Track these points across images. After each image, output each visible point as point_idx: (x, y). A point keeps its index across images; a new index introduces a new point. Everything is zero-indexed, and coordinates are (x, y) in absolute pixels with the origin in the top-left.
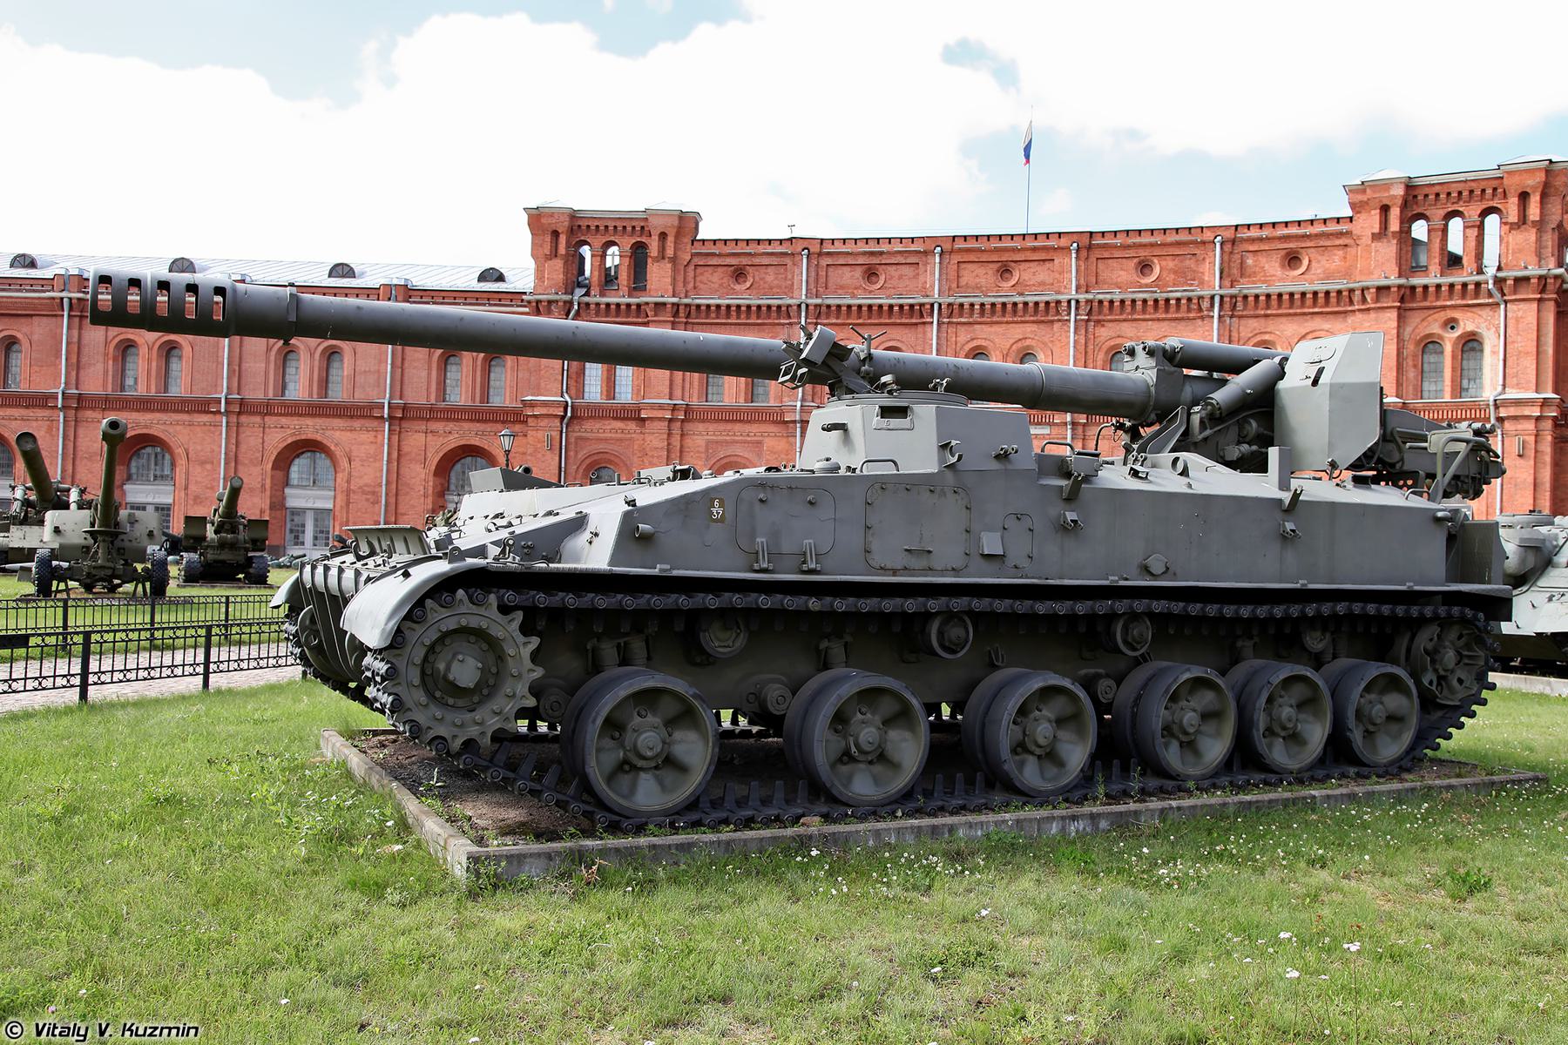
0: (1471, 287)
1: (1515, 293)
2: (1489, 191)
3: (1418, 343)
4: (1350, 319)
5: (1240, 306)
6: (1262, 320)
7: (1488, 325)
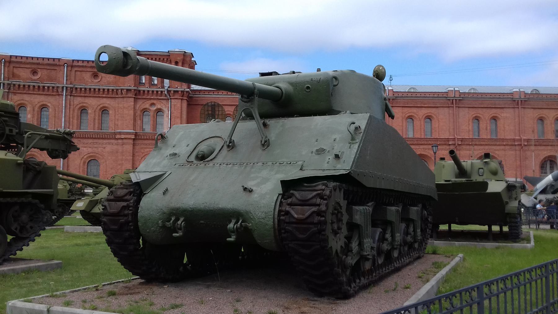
0: (159, 92)
1: (174, 96)
2: (165, 59)
3: (141, 111)
4: (117, 100)
5: (74, 91)
6: (83, 98)
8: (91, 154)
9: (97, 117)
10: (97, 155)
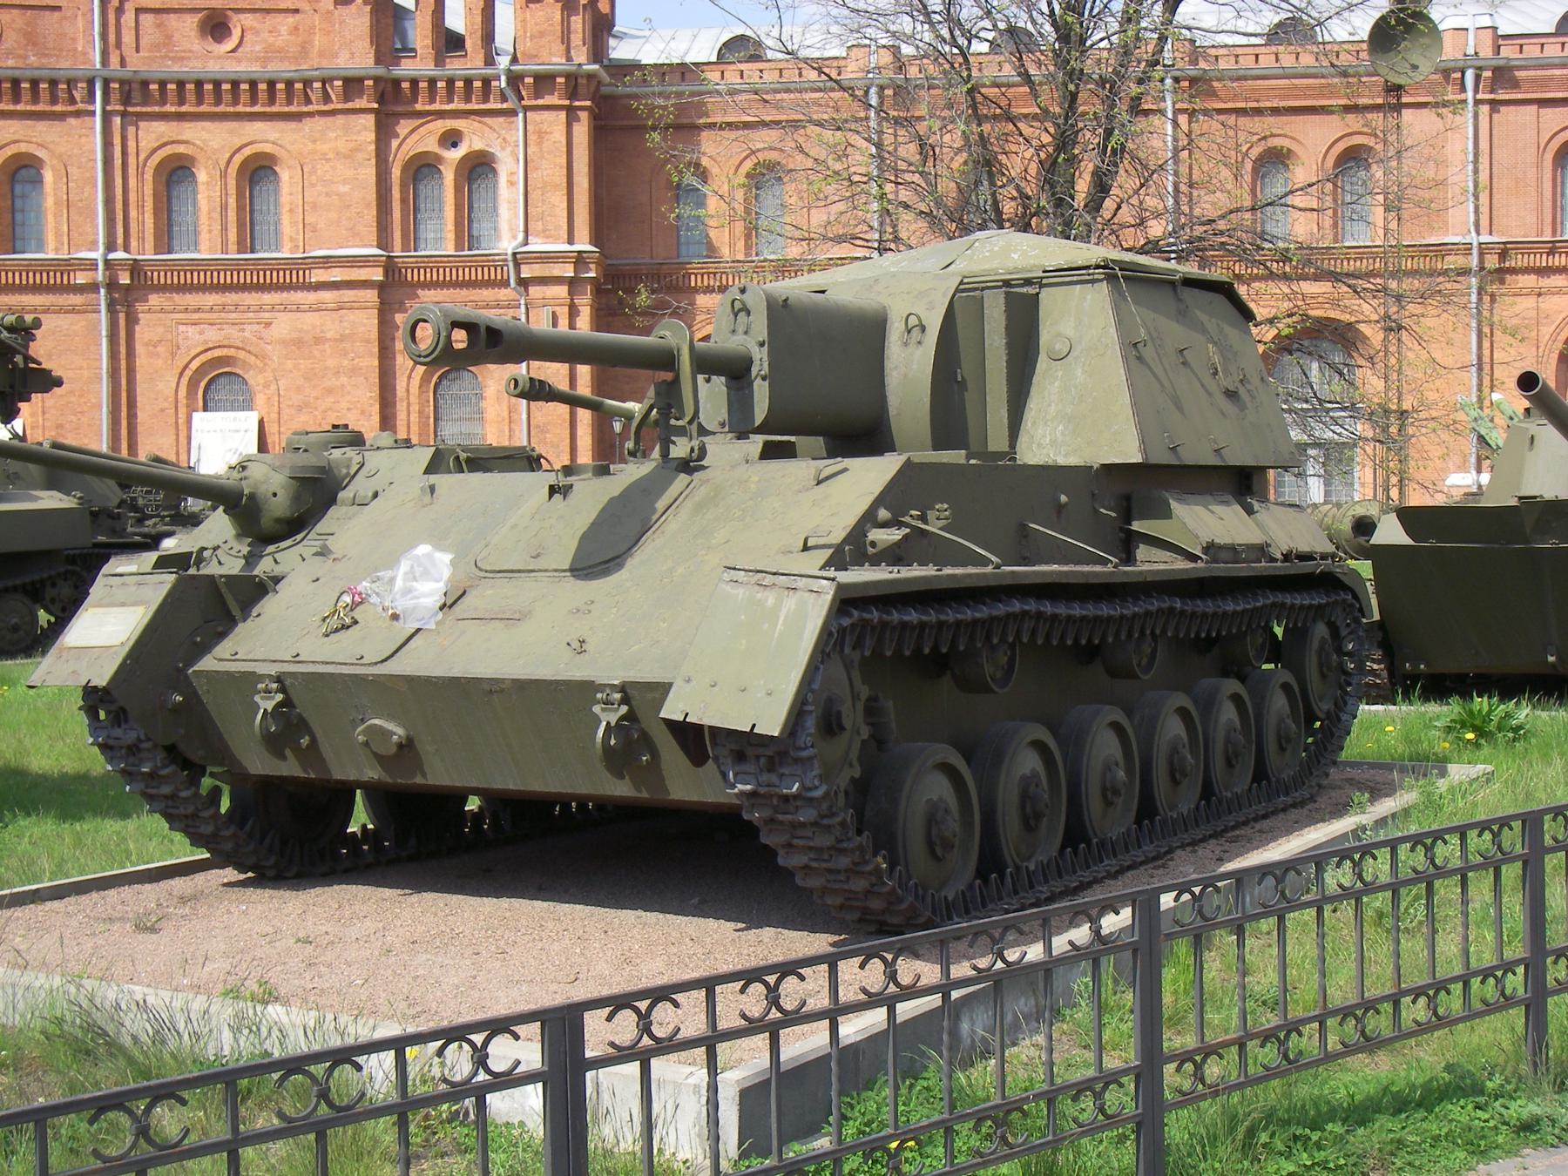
4: (308, 124)
5: (136, 96)
7: (501, 140)
8: (217, 353)
9: (232, 201)
10: (241, 355)
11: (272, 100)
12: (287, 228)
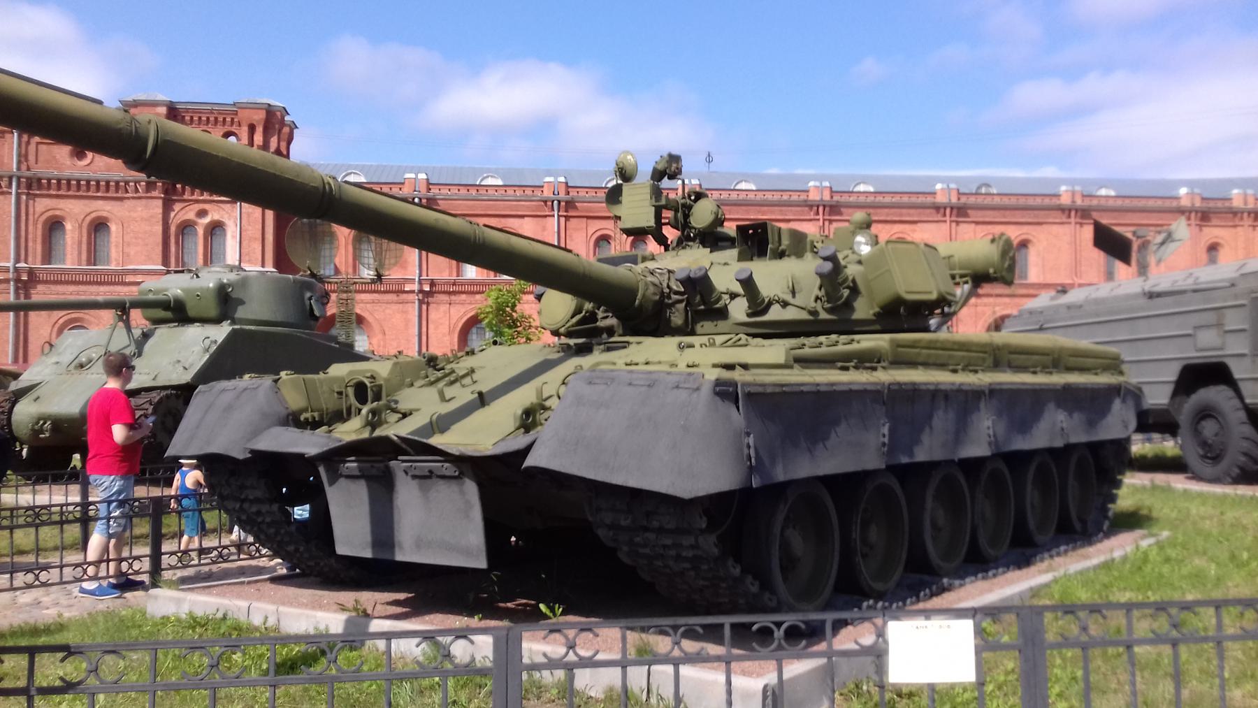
4: (128, 203)
5: (35, 185)
9: (85, 239)
11: (107, 190)
12: (114, 253)
